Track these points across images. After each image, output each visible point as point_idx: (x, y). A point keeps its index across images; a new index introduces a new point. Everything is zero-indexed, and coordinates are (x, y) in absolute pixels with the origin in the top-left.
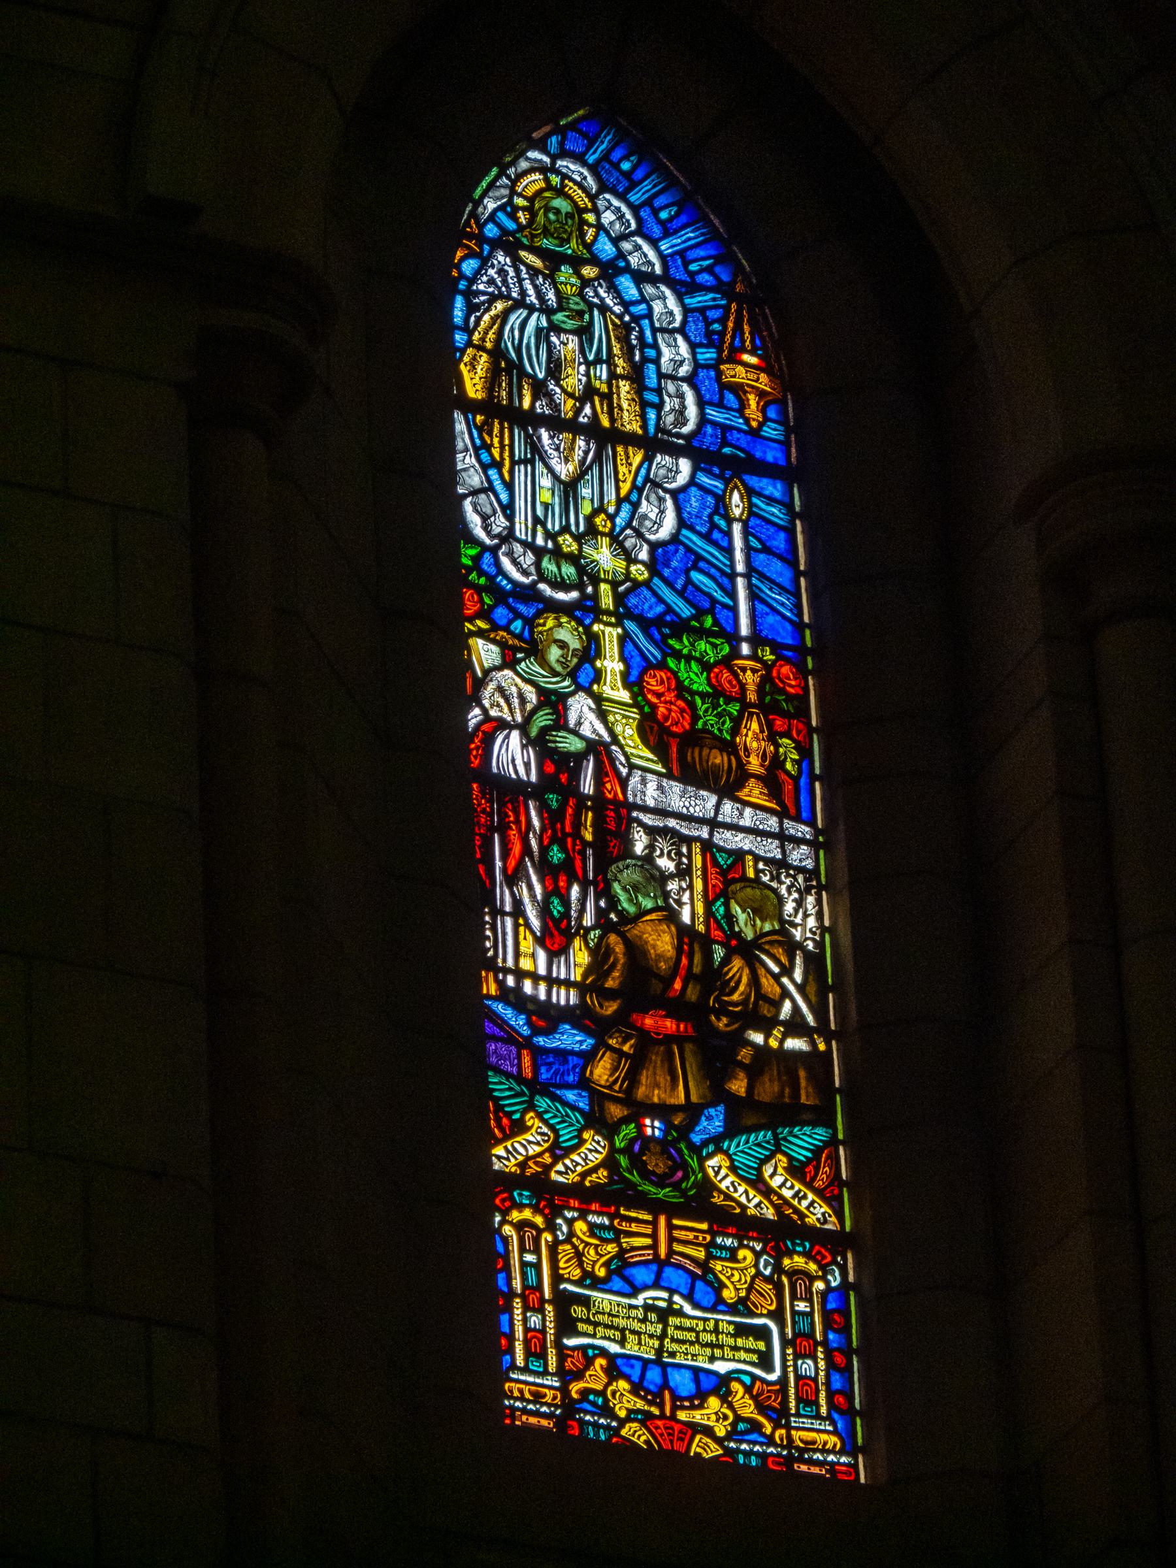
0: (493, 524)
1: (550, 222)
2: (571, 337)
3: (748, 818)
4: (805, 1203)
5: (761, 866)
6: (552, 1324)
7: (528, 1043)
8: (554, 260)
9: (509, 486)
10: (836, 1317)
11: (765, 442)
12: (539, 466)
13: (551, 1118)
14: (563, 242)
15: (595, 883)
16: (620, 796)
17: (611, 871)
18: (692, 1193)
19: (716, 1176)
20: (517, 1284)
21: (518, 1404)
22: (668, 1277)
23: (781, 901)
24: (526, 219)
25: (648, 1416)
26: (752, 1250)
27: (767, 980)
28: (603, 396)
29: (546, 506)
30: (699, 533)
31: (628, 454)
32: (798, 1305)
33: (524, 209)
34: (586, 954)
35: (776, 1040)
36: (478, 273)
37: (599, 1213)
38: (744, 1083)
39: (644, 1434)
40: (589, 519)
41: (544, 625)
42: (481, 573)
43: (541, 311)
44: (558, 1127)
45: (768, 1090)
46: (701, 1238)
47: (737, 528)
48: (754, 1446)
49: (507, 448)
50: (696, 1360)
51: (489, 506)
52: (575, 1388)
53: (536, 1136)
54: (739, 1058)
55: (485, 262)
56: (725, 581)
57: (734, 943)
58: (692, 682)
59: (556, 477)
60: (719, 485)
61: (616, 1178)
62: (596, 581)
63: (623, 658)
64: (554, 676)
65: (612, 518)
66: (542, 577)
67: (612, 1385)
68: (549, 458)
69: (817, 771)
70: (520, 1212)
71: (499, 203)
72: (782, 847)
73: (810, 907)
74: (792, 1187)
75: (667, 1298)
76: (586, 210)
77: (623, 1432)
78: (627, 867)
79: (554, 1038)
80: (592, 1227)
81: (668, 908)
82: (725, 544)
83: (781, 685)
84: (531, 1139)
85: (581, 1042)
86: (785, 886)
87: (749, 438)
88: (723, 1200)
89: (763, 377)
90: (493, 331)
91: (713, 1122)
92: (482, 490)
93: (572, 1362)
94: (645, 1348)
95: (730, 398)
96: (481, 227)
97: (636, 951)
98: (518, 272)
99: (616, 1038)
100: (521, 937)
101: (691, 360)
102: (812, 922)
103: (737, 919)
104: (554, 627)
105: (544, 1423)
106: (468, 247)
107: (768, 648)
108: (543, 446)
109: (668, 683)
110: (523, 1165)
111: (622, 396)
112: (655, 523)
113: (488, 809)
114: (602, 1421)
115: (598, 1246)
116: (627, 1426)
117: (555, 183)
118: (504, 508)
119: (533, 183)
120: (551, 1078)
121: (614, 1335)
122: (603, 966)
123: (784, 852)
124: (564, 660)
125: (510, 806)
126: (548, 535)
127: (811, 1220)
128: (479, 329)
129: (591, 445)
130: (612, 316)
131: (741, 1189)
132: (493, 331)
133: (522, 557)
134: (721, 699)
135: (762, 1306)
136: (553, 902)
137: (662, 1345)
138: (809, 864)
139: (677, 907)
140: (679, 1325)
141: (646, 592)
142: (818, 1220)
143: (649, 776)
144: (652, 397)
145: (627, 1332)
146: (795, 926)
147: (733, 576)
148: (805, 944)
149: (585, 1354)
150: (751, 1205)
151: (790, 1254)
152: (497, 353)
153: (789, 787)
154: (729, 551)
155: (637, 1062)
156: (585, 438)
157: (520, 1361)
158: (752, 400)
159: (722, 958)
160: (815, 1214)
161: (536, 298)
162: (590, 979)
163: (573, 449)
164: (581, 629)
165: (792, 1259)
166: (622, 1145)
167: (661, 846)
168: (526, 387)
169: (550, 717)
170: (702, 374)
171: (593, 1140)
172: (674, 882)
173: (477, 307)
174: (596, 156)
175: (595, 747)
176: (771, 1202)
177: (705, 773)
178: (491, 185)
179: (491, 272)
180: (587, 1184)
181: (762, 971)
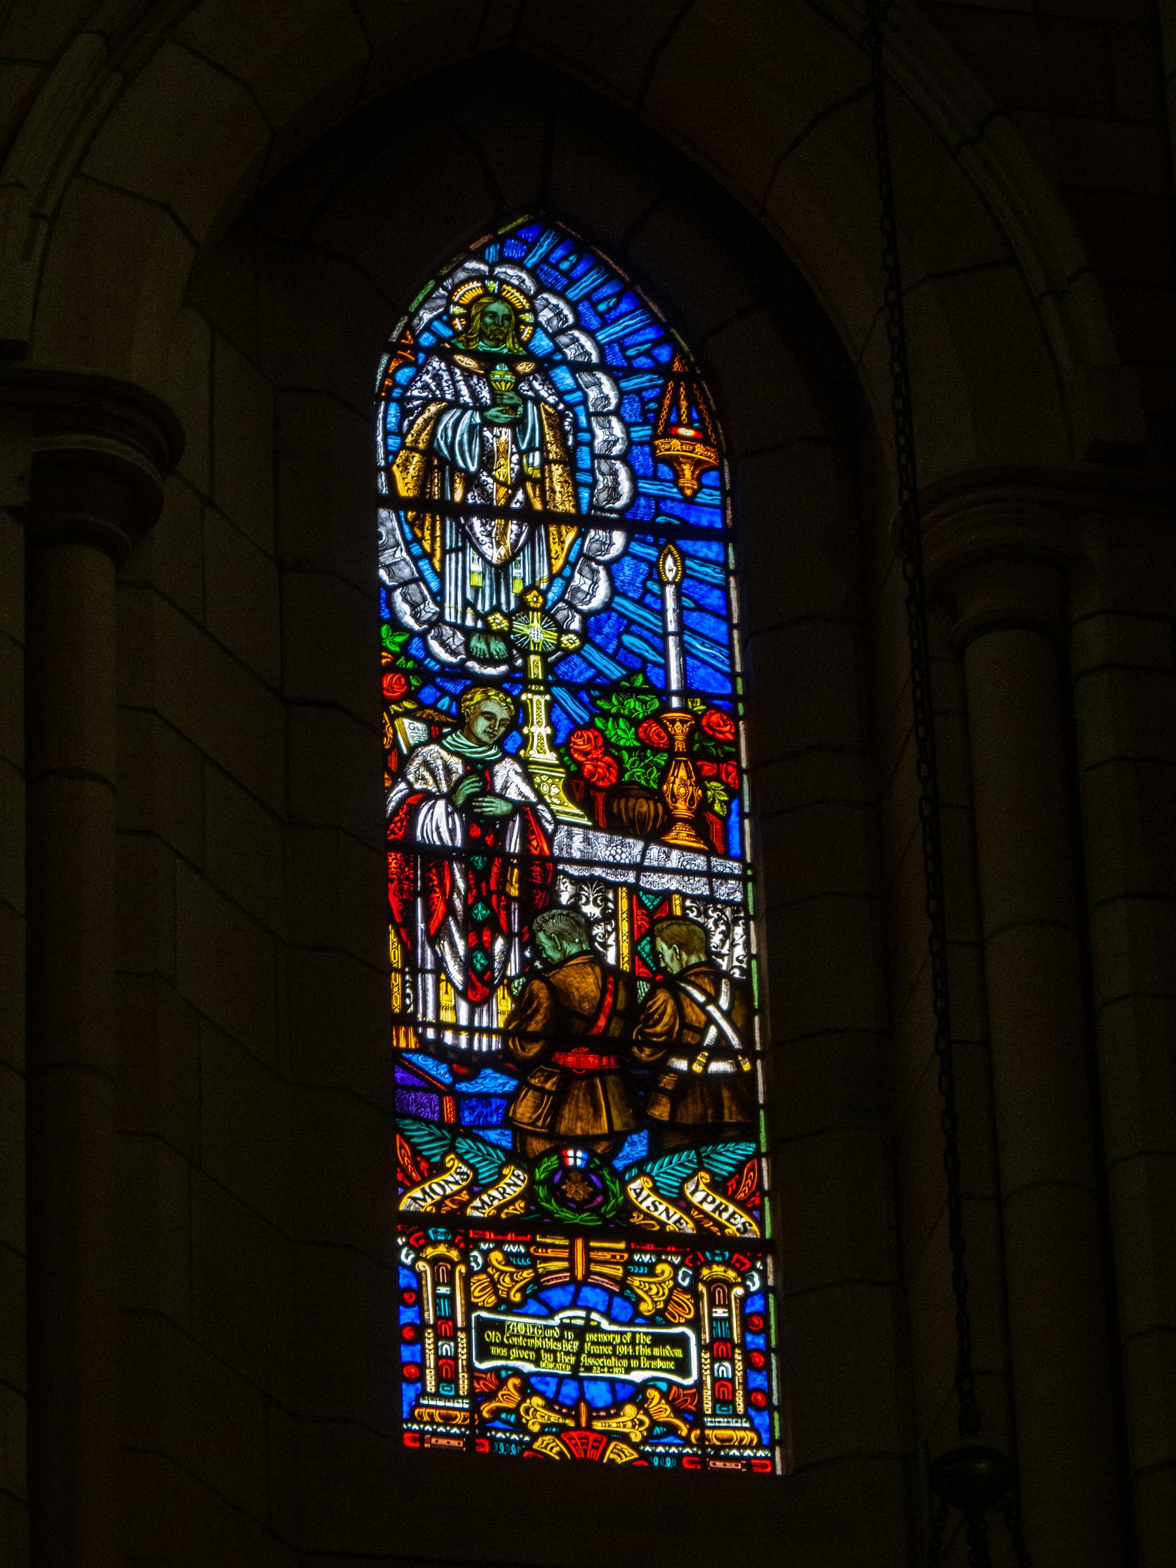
0: (423, 611)
1: (486, 325)
2: (504, 430)
3: (675, 860)
4: (725, 1215)
5: (688, 903)
6: (465, 1350)
7: (450, 1090)
8: (488, 361)
9: (441, 576)
10: (756, 1320)
11: (700, 507)
12: (470, 552)
13: (472, 1158)
14: (498, 342)
15: (520, 934)
16: (546, 850)
17: (537, 922)
18: (611, 1215)
19: (637, 1199)
20: (430, 1316)
21: (428, 1428)
22: (586, 1297)
23: (708, 934)
24: (462, 325)
25: (563, 1428)
26: (671, 1264)
27: (693, 1009)
28: (535, 482)
29: (476, 589)
30: (632, 600)
31: (561, 532)
32: (716, 1312)
33: (460, 316)
34: (510, 1000)
35: (699, 1065)
36: (412, 381)
37: (514, 1243)
38: (667, 1109)
39: (557, 1445)
40: (521, 598)
41: (472, 699)
42: (409, 657)
43: (474, 409)
44: (477, 1166)
45: (691, 1112)
46: (618, 1257)
47: (670, 591)
48: (670, 1448)
49: (438, 539)
50: (612, 1372)
51: (419, 595)
52: (486, 1409)
53: (455, 1176)
54: (662, 1085)
55: (420, 369)
56: (657, 641)
57: (659, 978)
58: (619, 738)
59: (487, 562)
60: (653, 552)
61: (533, 1208)
62: (525, 653)
63: (550, 722)
64: (481, 746)
65: (544, 594)
66: (471, 656)
67: (525, 1402)
68: (481, 544)
69: (747, 810)
70: (435, 1248)
71: (435, 313)
72: (710, 884)
73: (737, 937)
74: (714, 1201)
75: (584, 1316)
76: (524, 311)
77: (536, 1446)
78: (553, 917)
79: (477, 1083)
80: (508, 1256)
81: (593, 950)
82: (657, 607)
83: (711, 733)
84: (451, 1179)
85: (504, 1085)
86: (713, 919)
87: (683, 505)
88: (643, 1220)
89: (699, 448)
90: (426, 432)
91: (637, 1146)
92: (414, 581)
93: (484, 1384)
94: (561, 1364)
95: (664, 470)
96: (416, 338)
97: (558, 994)
98: (452, 374)
99: (539, 1077)
100: (442, 992)
101: (625, 439)
102: (739, 951)
103: (663, 956)
104: (482, 700)
105: (454, 1443)
106: (402, 357)
107: (698, 700)
108: (474, 534)
109: (595, 742)
110: (438, 1205)
111: (554, 479)
112: (588, 594)
113: (411, 876)
114: (514, 1437)
115: (514, 1273)
116: (540, 1440)
117: (492, 289)
118: (434, 596)
119: (471, 290)
120: (475, 1121)
121: (529, 1355)
122: (527, 1012)
123: (711, 889)
124: (491, 731)
125: (434, 871)
126: (478, 616)
127: (731, 1230)
128: (412, 432)
129: (524, 528)
130: (546, 407)
131: (661, 1208)
132: (426, 432)
133: (451, 639)
134: (649, 751)
135: (679, 1316)
136: (476, 956)
137: (578, 1361)
138: (738, 897)
139: (601, 949)
140: (596, 1340)
141: (576, 659)
142: (738, 1230)
143: (576, 830)
144: (584, 478)
145: (542, 1351)
146: (722, 956)
147: (665, 636)
148: (732, 972)
149: (498, 1376)
150: (670, 1222)
151: (709, 1264)
152: (430, 452)
153: (717, 827)
154: (661, 613)
155: (560, 1099)
156: (518, 521)
157: (431, 1387)
158: (687, 470)
159: (646, 994)
160: (735, 1225)
161: (470, 397)
162: (513, 1025)
163: (505, 534)
164: (509, 700)
165: (710, 1268)
166: (543, 1176)
167: (587, 894)
168: (458, 481)
169: (477, 784)
170: (636, 450)
171: (513, 1174)
172: (599, 927)
173: (410, 412)
174: (535, 259)
175: (523, 809)
176: (691, 1218)
177: (631, 822)
178: (428, 298)
179: (426, 378)
180: (503, 1216)
181: (686, 1002)
